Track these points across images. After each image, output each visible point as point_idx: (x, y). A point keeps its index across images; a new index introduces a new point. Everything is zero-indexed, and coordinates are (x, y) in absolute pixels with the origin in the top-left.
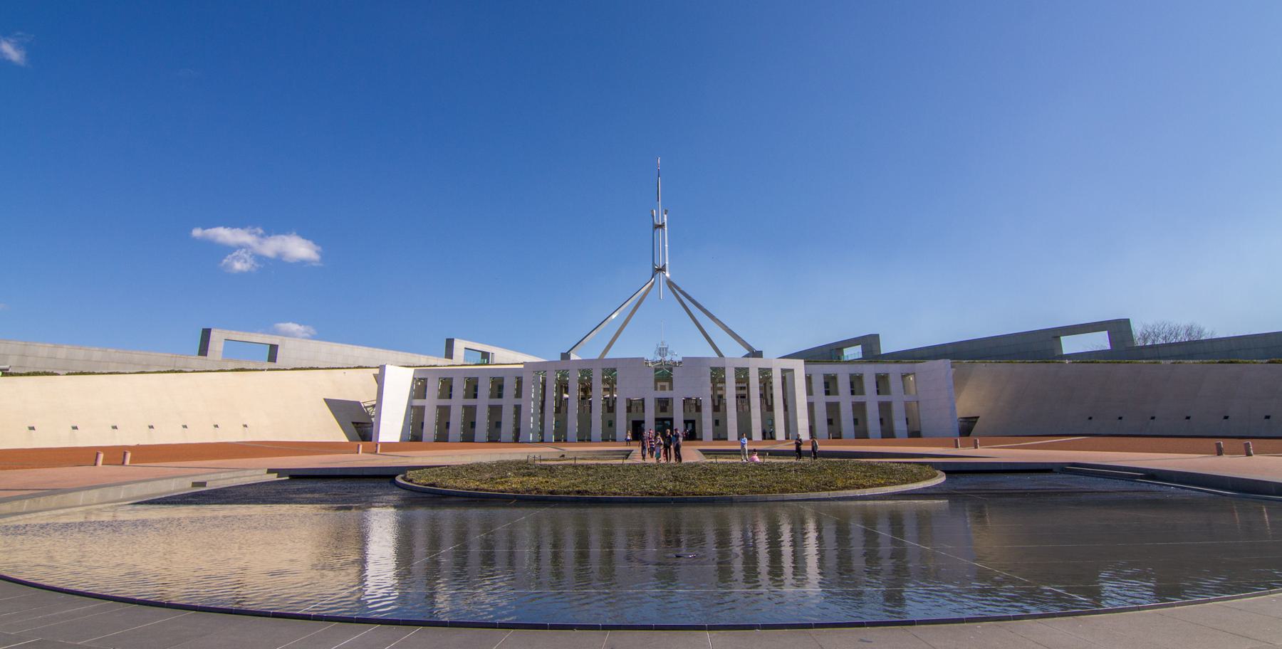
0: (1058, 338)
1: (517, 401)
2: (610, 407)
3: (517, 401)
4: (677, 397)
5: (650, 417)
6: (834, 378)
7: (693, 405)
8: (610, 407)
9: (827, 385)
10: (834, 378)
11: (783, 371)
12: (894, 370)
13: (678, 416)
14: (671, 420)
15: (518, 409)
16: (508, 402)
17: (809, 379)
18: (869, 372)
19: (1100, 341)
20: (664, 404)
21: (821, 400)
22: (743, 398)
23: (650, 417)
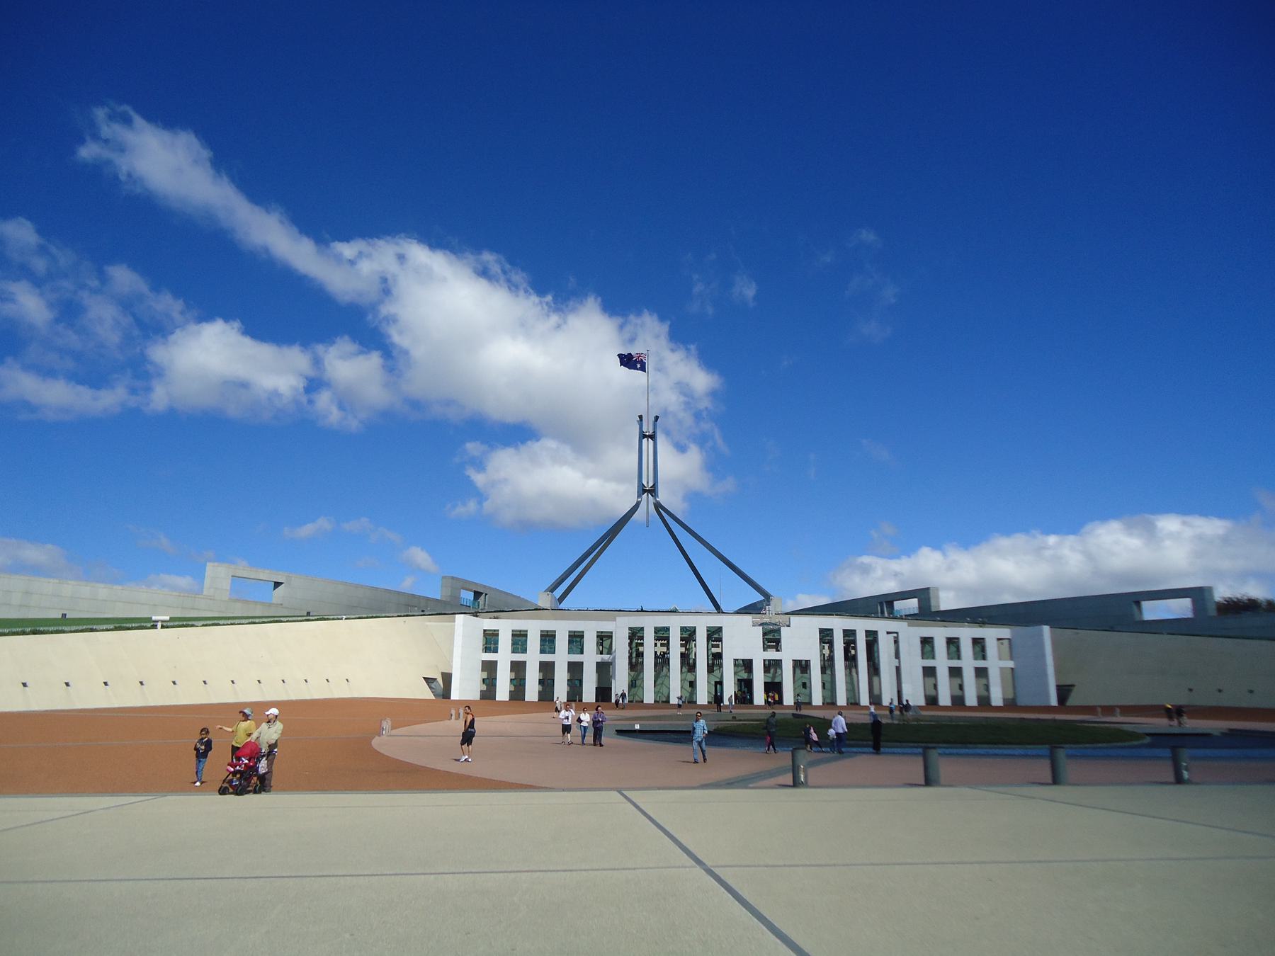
0: (1138, 603)
4: (787, 656)
7: (802, 667)
9: (983, 649)
11: (868, 633)
17: (927, 642)
20: (772, 666)
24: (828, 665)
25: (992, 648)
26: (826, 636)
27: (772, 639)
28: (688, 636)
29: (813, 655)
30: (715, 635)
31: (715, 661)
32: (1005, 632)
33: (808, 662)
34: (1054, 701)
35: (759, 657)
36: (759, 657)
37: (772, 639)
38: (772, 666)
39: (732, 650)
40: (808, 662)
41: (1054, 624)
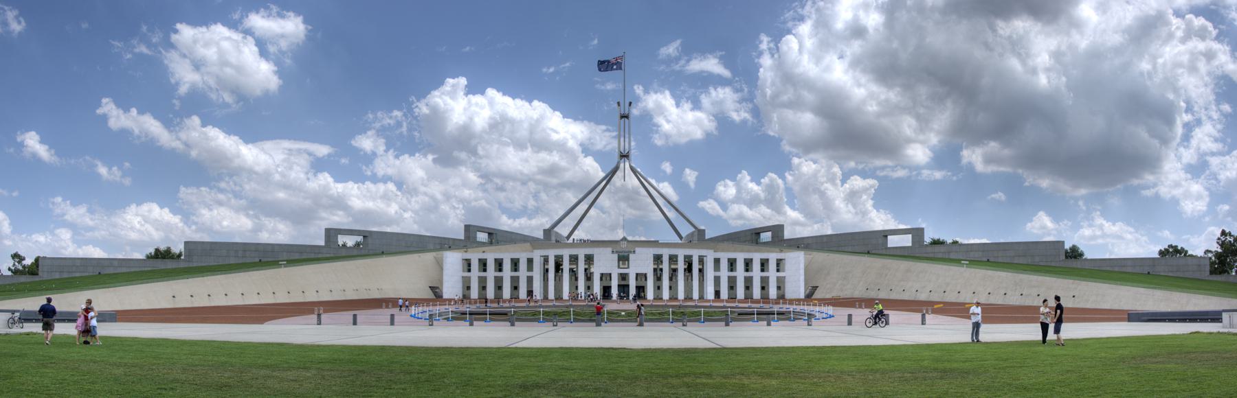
1: (530, 274)
2: (589, 277)
3: (530, 274)
5: (614, 284)
6: (735, 260)
7: (641, 277)
8: (589, 277)
10: (735, 260)
12: (773, 257)
13: (632, 284)
14: (628, 286)
15: (530, 280)
16: (523, 273)
17: (717, 261)
18: (757, 257)
19: (906, 241)
21: (724, 273)
22: (674, 272)
23: (614, 284)
26: (658, 259)
27: (624, 259)
29: (649, 269)
30: (589, 259)
33: (645, 276)
37: (624, 259)
38: (624, 277)
39: (597, 270)
40: (645, 276)
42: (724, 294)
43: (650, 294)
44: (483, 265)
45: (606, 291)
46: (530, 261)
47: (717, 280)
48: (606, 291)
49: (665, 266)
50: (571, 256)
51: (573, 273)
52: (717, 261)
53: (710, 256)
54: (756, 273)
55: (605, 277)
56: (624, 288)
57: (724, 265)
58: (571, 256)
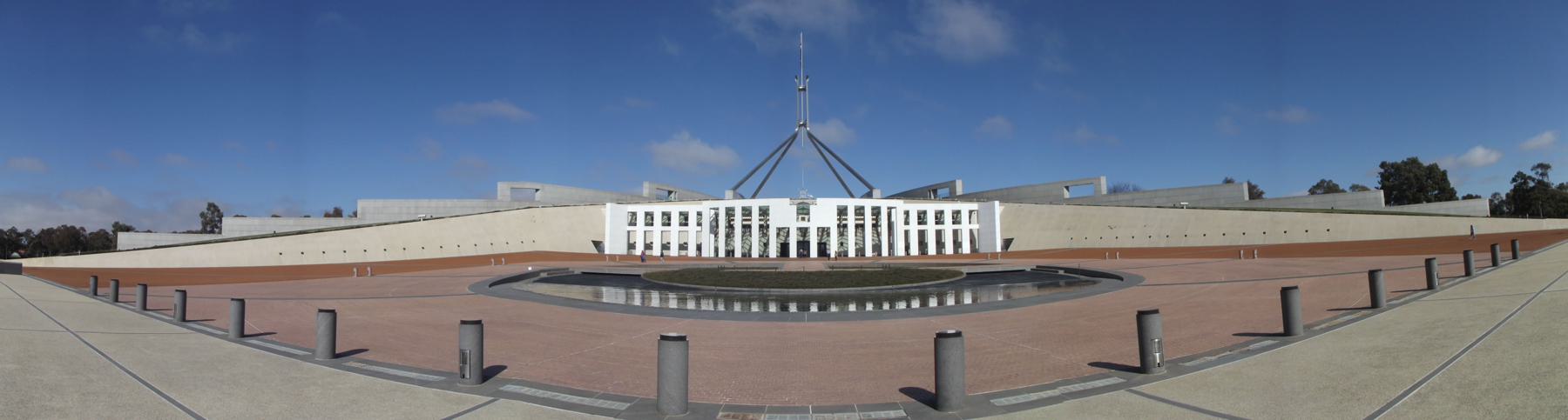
6: (925, 213)
7: (824, 232)
14: (808, 243)
17: (907, 213)
18: (948, 208)
20: (804, 232)
21: (914, 228)
24: (842, 227)
25: (965, 217)
26: (842, 212)
27: (803, 211)
28: (747, 212)
29: (832, 223)
30: (764, 212)
31: (764, 228)
32: (974, 206)
34: (999, 249)
35: (794, 225)
36: (794, 225)
37: (803, 211)
38: (804, 232)
39: (774, 225)
41: (1003, 200)
42: (914, 251)
43: (833, 249)
44: (649, 217)
45: (784, 249)
46: (699, 214)
47: (907, 233)
48: (784, 249)
49: (851, 221)
50: (744, 209)
51: (747, 228)
52: (907, 213)
53: (900, 205)
54: (948, 227)
55: (783, 232)
56: (804, 245)
57: (914, 218)
58: (744, 209)
